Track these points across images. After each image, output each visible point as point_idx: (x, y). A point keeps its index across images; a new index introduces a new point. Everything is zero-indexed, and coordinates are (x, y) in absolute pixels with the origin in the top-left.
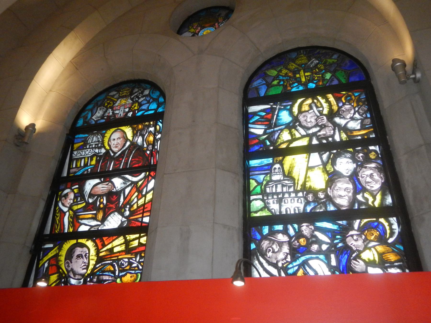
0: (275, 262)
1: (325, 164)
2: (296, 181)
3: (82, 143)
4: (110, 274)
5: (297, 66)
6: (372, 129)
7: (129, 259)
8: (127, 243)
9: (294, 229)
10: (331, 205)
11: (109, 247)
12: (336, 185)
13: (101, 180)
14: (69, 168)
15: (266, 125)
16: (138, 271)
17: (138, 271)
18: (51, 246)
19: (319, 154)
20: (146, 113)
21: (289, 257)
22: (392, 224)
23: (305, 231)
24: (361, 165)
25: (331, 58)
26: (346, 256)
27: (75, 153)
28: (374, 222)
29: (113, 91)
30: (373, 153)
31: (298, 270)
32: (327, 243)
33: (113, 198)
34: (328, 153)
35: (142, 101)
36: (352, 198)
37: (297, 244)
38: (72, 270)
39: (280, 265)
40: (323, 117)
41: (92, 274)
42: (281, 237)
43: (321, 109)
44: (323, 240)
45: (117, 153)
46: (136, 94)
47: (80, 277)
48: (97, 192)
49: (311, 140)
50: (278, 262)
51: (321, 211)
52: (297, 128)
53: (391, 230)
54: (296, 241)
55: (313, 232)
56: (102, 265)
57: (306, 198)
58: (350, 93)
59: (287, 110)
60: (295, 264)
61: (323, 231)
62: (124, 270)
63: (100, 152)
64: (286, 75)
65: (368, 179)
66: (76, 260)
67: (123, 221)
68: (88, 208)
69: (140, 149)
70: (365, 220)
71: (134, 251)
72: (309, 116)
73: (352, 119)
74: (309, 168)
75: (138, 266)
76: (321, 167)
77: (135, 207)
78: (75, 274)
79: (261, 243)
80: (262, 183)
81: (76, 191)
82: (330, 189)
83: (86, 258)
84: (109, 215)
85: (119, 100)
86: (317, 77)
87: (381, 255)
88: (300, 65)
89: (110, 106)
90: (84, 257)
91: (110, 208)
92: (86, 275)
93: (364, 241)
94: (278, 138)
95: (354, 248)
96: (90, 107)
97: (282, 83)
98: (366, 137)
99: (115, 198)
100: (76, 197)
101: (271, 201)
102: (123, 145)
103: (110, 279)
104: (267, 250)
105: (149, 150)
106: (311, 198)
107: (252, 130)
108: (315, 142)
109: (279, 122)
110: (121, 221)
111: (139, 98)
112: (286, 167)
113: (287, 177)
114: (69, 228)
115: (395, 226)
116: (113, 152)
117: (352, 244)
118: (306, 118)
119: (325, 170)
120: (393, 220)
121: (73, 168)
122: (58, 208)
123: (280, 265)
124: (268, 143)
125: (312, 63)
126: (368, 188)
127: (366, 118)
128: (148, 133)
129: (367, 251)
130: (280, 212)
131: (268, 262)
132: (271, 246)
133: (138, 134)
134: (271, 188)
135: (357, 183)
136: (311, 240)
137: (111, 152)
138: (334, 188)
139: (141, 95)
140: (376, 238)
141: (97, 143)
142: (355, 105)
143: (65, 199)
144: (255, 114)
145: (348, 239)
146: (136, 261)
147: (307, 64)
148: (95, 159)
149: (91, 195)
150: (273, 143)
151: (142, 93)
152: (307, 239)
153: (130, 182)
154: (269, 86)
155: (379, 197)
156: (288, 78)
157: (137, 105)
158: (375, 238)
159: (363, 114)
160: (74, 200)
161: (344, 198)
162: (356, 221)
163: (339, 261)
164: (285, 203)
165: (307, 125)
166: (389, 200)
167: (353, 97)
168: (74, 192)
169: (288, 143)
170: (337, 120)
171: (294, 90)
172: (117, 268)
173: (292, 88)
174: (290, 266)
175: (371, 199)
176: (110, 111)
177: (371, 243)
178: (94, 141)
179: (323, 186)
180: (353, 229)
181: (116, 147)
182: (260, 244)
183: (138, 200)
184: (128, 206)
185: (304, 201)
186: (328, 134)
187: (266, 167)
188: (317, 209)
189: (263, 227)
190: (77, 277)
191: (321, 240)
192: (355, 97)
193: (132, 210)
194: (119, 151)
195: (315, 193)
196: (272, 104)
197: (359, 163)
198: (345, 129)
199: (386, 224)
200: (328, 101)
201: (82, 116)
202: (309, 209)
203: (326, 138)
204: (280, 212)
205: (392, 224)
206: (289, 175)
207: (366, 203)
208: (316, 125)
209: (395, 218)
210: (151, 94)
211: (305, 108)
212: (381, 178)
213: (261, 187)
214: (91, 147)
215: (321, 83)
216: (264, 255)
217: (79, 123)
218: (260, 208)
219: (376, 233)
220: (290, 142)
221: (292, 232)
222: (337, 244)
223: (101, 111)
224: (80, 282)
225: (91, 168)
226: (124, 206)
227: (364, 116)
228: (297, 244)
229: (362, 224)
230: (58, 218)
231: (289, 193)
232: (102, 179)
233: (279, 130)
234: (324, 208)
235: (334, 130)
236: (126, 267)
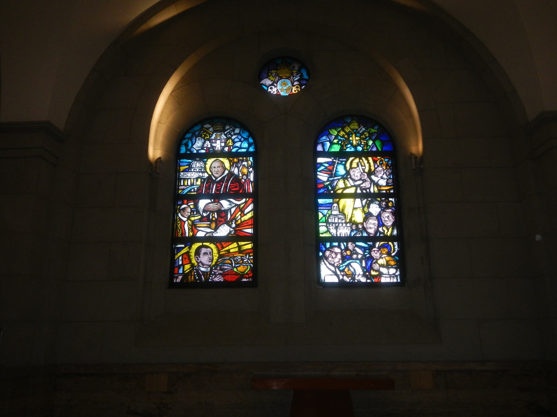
1: (363, 207)
2: (346, 216)
3: (188, 167)
4: (229, 265)
5: (350, 130)
6: (392, 187)
7: (241, 257)
8: (239, 247)
9: (344, 245)
10: (365, 233)
11: (227, 248)
12: (369, 221)
13: (211, 200)
15: (329, 174)
16: (248, 264)
17: (248, 264)
18: (183, 246)
20: (239, 151)
21: (341, 261)
22: (395, 246)
24: (383, 210)
25: (373, 128)
26: (370, 262)
27: (182, 174)
28: (386, 244)
29: (207, 124)
30: (391, 203)
31: (345, 268)
32: (361, 254)
33: (222, 214)
35: (235, 139)
36: (376, 229)
37: (346, 254)
38: (201, 262)
39: (336, 265)
40: (365, 174)
41: (216, 264)
42: (337, 250)
43: (364, 168)
45: (218, 178)
46: (228, 131)
47: (207, 267)
48: (209, 209)
49: (356, 190)
50: (334, 263)
52: (349, 180)
53: (394, 248)
55: (354, 248)
56: (222, 260)
57: (351, 227)
58: (382, 159)
59: (343, 164)
60: (344, 265)
61: (360, 247)
62: (238, 263)
63: (203, 175)
64: (343, 136)
65: (386, 219)
66: (203, 256)
67: (231, 230)
68: (203, 220)
69: (237, 179)
70: (382, 243)
71: (245, 252)
72: (357, 171)
73: (382, 178)
74: (354, 209)
75: (247, 261)
76: (361, 208)
77: (239, 222)
78: (203, 264)
80: (326, 215)
81: (192, 207)
82: (366, 223)
83: (211, 255)
84: (220, 226)
85: (215, 134)
86: (363, 142)
87: (387, 262)
88: (353, 130)
89: (207, 138)
90: (209, 254)
91: (220, 221)
92: (212, 265)
93: (380, 254)
94: (336, 185)
95: (375, 258)
96: (188, 135)
97: (340, 142)
98: (388, 192)
99: (223, 214)
100: (192, 211)
101: (331, 227)
102: (222, 173)
103: (229, 268)
104: (328, 256)
105: (244, 179)
106: (354, 227)
107: (319, 177)
108: (359, 191)
109: (338, 173)
110: (230, 230)
111: (232, 136)
112: (341, 207)
115: (396, 247)
116: (214, 177)
118: (354, 173)
120: (396, 243)
121: (181, 186)
122: (178, 218)
123: (336, 265)
124: (330, 188)
125: (361, 129)
126: (386, 224)
127: (390, 178)
128: (242, 166)
129: (381, 259)
133: (234, 166)
134: (331, 219)
135: (380, 221)
137: (213, 177)
138: (367, 223)
139: (233, 132)
141: (201, 168)
142: (385, 168)
143: (184, 212)
144: (321, 164)
145: (372, 253)
146: (246, 258)
147: (358, 129)
148: (199, 180)
149: (204, 211)
150: (334, 188)
151: (234, 131)
152: (351, 251)
153: (235, 204)
154: (332, 143)
155: (390, 230)
156: (345, 139)
157: (231, 141)
160: (191, 213)
161: (373, 229)
163: (366, 264)
164: (339, 229)
165: (354, 178)
166: (395, 232)
167: (384, 162)
168: (190, 208)
169: (342, 190)
171: (348, 150)
172: (233, 262)
173: (347, 148)
175: (386, 231)
176: (208, 142)
178: (197, 166)
180: (375, 247)
181: (217, 173)
183: (241, 217)
184: (234, 221)
185: (350, 229)
186: (367, 186)
187: (329, 205)
189: (327, 243)
190: (205, 266)
192: (385, 162)
193: (237, 223)
194: (219, 177)
195: (357, 224)
196: (333, 158)
197: (383, 209)
198: (377, 184)
199: (392, 245)
200: (368, 162)
201: (183, 143)
202: (353, 234)
203: (366, 189)
204: (337, 235)
205: (395, 246)
206: (343, 212)
207: (383, 233)
208: (360, 179)
209: (397, 243)
210: (241, 133)
211: (354, 165)
212: (393, 219)
213: (325, 218)
214: (195, 171)
215: (365, 148)
216: (327, 259)
217: (181, 149)
218: (325, 231)
219: (386, 250)
221: (343, 247)
222: (367, 255)
223: (200, 141)
224: (208, 270)
225: (197, 187)
226: (231, 220)
227: (389, 177)
228: (346, 254)
229: (380, 245)
230: (179, 225)
231: (342, 224)
232: (212, 200)
233: (337, 179)
234: (361, 234)
235: (371, 184)
236: (240, 261)
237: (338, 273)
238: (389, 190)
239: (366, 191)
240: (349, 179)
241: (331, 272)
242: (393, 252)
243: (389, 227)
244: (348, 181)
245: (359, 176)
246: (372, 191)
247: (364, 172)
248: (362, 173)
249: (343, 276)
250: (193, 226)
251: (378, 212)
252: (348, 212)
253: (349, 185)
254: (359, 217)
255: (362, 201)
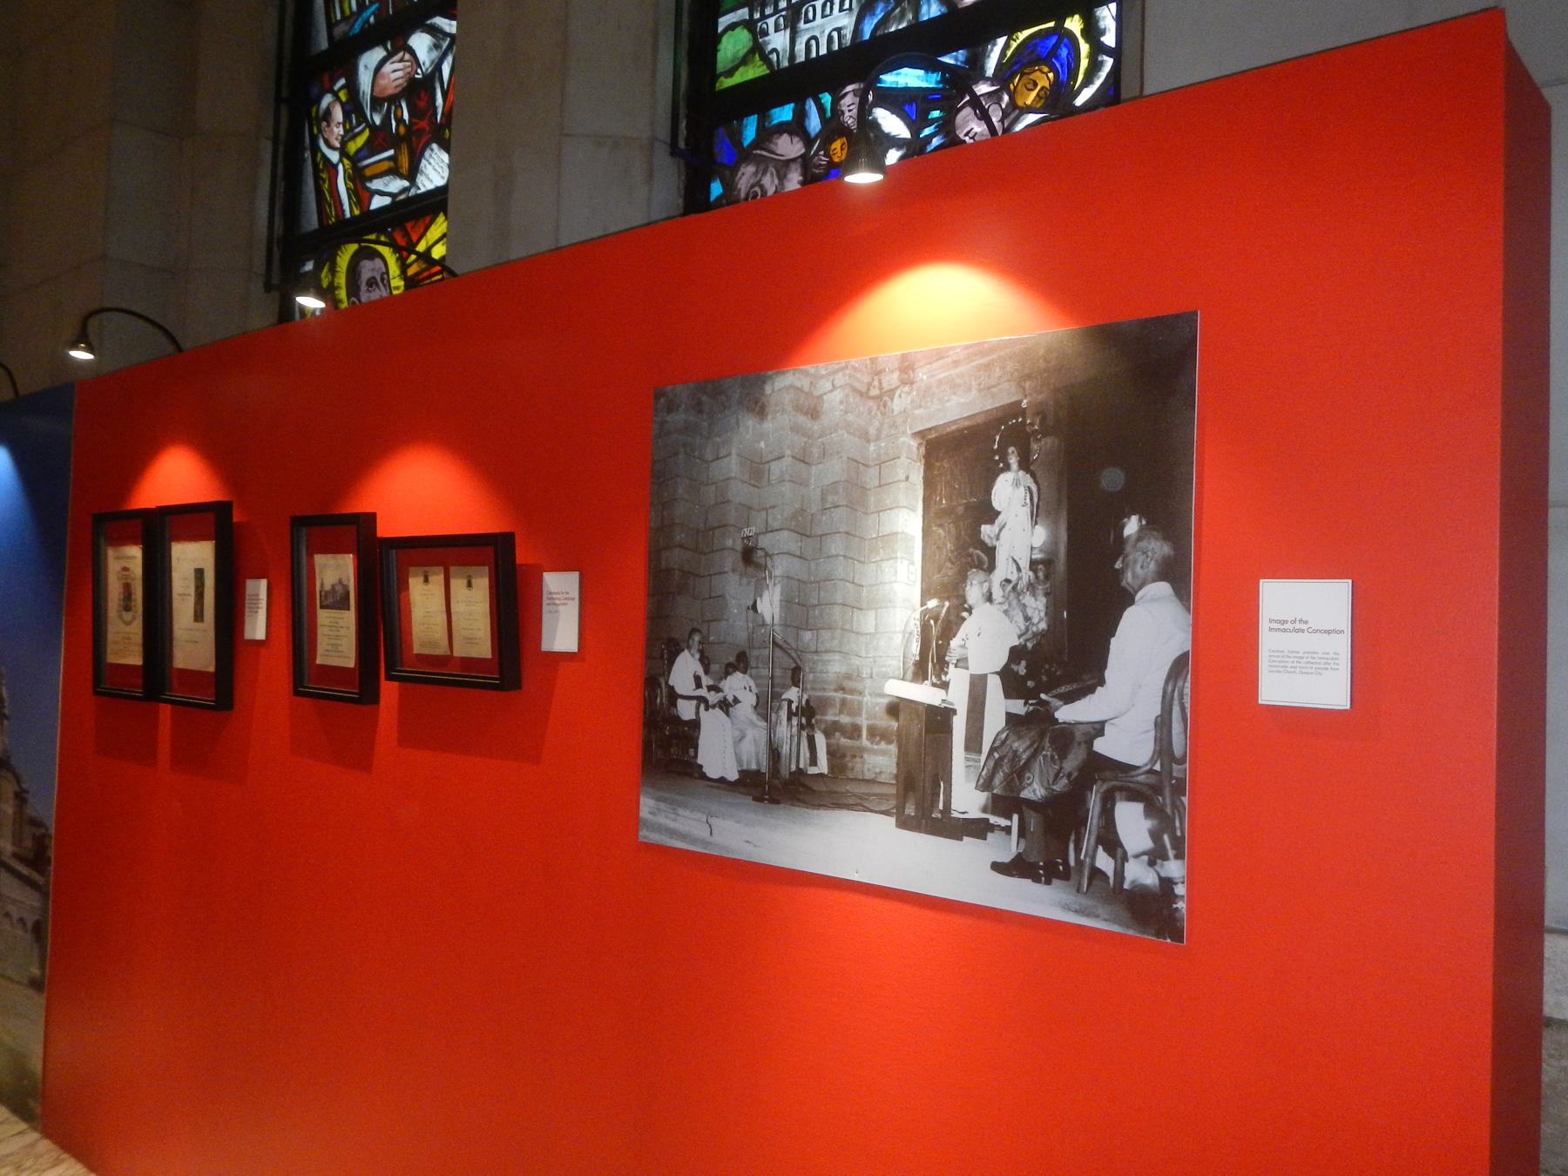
9: (821, 109)
14: (331, 26)
23: (850, 111)
42: (789, 147)
44: (893, 134)
51: (900, 27)
54: (822, 153)
61: (898, 100)
70: (1023, 35)
79: (736, 175)
114: (351, 211)
117: (967, 135)
121: (338, 23)
122: (319, 155)
130: (792, 56)
132: (760, 180)
140: (1041, 98)
149: (376, 102)
158: (1038, 99)
162: (995, 45)
177: (1023, 119)
180: (981, 77)
182: (734, 179)
188: (892, 21)
191: (887, 136)
221: (814, 124)
225: (373, 13)
242: (1088, 81)
250: (359, 179)
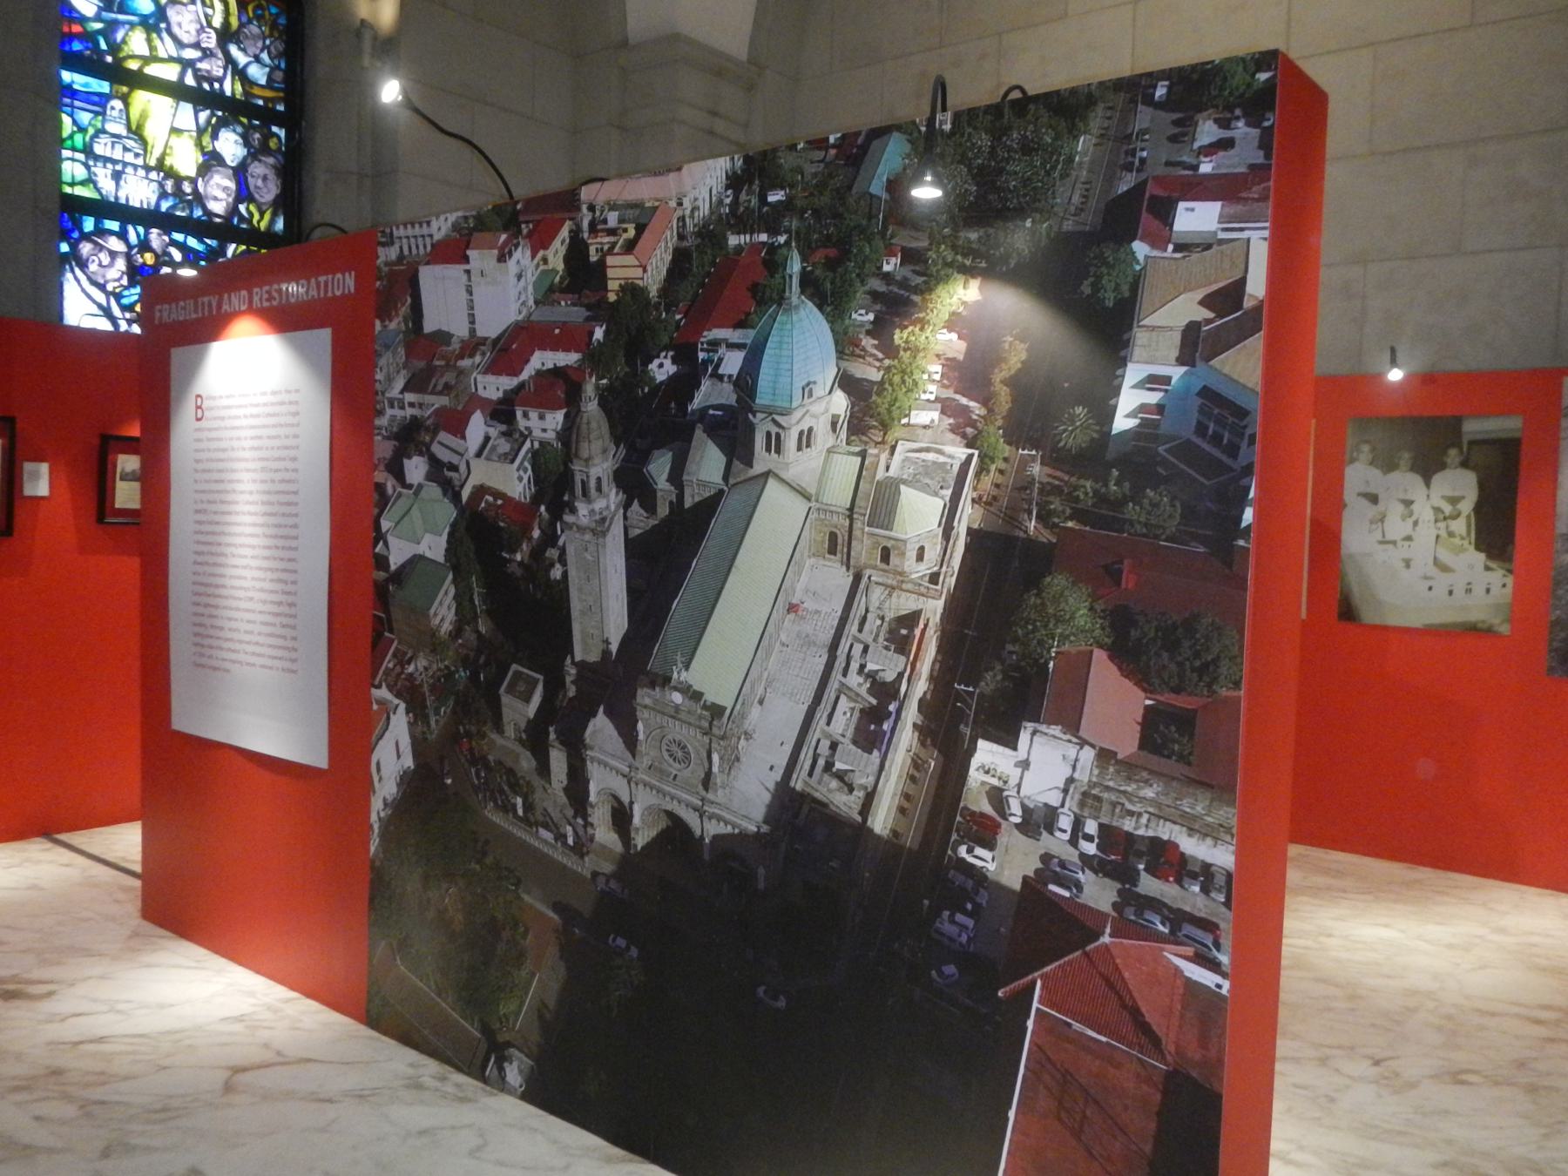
0: (102, 281)
1: (201, 132)
6: (281, 94)
9: (138, 235)
12: (212, 177)
19: (194, 108)
21: (125, 278)
30: (275, 140)
34: (208, 112)
37: (141, 260)
42: (115, 244)
50: (106, 282)
57: (161, 186)
61: (182, 247)
73: (257, 59)
76: (195, 134)
98: (270, 105)
104: (87, 260)
108: (190, 80)
112: (135, 113)
113: (135, 133)
119: (199, 144)
123: (110, 287)
124: (103, 46)
126: (257, 196)
127: (278, 67)
131: (89, 279)
136: (162, 259)
138: (208, 181)
142: (267, 33)
150: (115, 48)
155: (267, 216)
159: (275, 57)
166: (280, 225)
167: (267, 13)
170: (233, 50)
174: (126, 293)
175: (256, 217)
179: (193, 173)
187: (96, 99)
192: (271, 14)
195: (179, 180)
198: (241, 74)
202: (165, 206)
203: (211, 80)
204: (117, 198)
207: (249, 221)
208: (197, 46)
216: (83, 265)
220: (147, 60)
229: (238, 252)
235: (225, 69)
237: (116, 311)
238: (272, 100)
239: (211, 85)
240: (165, 35)
241: (95, 307)
243: (264, 208)
244: (162, 39)
245: (194, 33)
246: (228, 93)
247: (210, 25)
248: (202, 27)
249: (130, 322)
251: (241, 157)
252: (155, 133)
253: (162, 54)
254: (186, 160)
255: (196, 114)
